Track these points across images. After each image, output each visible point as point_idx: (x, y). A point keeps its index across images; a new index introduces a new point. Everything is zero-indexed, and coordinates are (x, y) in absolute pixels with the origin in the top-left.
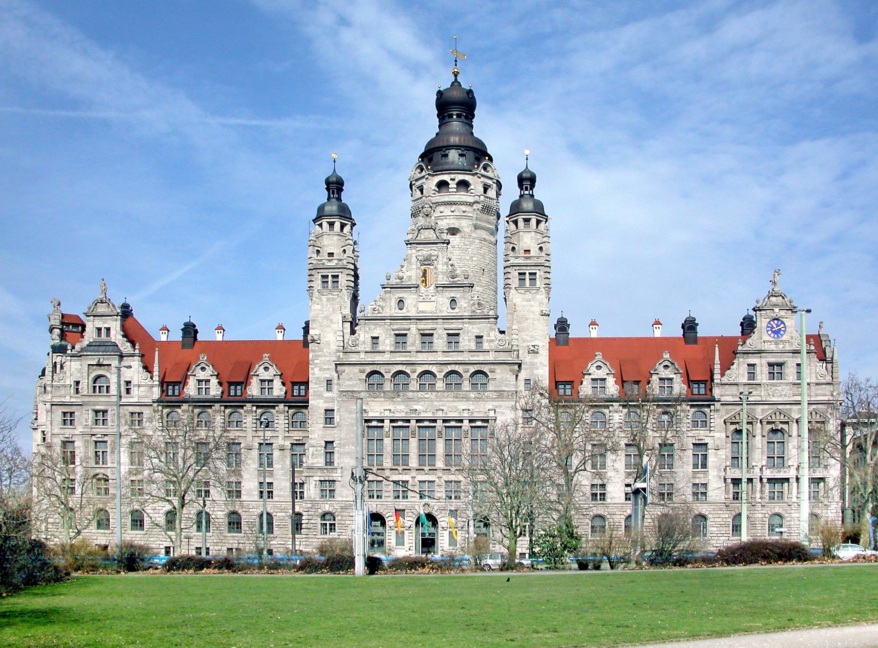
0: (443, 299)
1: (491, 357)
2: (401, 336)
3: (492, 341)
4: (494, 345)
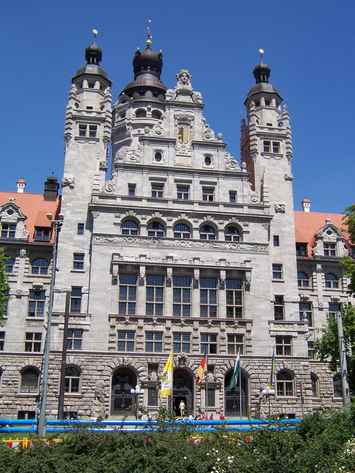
1: (246, 211)
2: (158, 187)
3: (246, 196)
4: (247, 201)
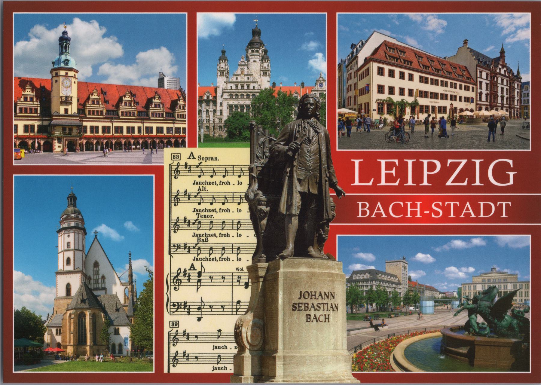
0: (246, 78)
1: (257, 91)
2: (237, 86)
